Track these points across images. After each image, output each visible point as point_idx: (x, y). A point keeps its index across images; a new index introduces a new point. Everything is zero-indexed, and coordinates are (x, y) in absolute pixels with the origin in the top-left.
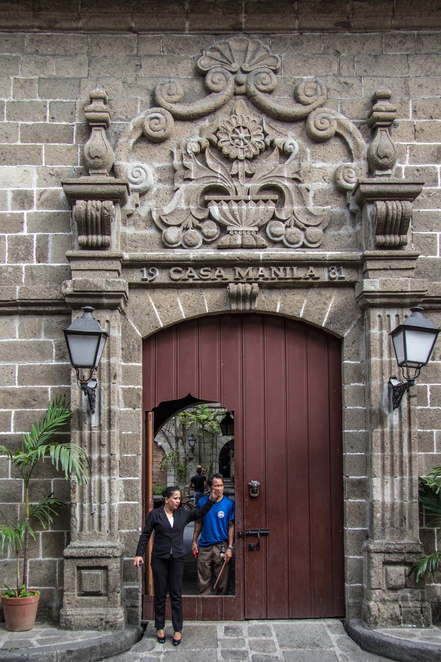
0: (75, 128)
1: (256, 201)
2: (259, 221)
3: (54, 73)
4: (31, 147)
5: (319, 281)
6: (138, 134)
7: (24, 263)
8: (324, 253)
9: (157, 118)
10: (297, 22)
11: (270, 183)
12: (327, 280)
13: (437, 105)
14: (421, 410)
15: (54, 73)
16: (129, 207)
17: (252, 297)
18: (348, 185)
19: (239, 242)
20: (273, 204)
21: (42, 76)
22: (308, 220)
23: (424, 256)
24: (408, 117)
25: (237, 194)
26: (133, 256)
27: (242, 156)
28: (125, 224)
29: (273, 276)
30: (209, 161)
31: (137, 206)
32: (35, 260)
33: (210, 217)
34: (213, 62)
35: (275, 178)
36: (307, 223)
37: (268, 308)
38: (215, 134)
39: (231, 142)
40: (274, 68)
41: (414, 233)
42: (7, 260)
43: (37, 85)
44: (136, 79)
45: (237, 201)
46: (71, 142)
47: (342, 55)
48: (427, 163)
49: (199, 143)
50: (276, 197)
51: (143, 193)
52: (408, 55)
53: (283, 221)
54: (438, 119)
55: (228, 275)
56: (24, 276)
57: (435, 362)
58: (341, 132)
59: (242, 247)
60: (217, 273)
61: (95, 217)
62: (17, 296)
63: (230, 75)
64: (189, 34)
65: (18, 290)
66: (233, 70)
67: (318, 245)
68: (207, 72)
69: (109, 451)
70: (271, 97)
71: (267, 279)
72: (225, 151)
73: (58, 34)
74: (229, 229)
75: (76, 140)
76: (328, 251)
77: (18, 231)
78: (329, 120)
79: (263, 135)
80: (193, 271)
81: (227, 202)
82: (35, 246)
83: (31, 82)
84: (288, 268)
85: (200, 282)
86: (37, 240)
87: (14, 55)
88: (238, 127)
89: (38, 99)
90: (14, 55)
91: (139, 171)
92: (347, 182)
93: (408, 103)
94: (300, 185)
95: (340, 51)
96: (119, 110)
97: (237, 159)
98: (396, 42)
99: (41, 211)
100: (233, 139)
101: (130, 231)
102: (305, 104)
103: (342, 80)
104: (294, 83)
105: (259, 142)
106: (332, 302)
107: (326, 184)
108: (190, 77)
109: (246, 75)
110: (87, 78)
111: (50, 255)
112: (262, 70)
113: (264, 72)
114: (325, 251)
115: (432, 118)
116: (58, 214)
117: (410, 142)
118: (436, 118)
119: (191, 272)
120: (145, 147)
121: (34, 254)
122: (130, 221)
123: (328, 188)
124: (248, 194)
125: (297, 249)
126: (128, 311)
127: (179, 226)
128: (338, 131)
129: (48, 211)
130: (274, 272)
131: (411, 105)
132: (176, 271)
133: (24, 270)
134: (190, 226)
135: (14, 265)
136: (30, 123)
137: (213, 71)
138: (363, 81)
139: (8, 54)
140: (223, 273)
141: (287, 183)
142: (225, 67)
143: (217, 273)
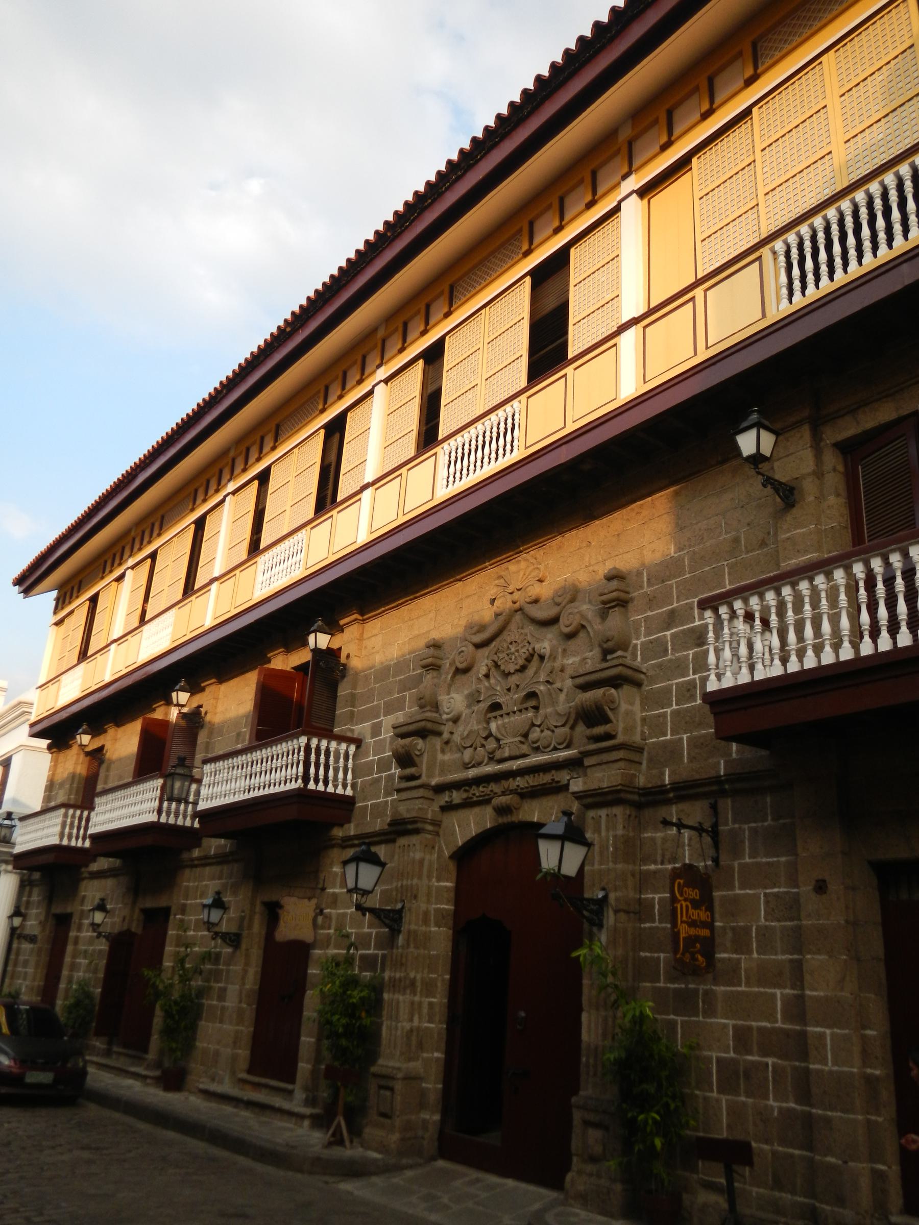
1: (520, 711)
2: (521, 731)
5: (561, 784)
6: (453, 669)
9: (462, 651)
13: (667, 567)
14: (650, 928)
15: (417, 632)
16: (446, 736)
19: (507, 754)
20: (533, 710)
23: (655, 740)
27: (512, 671)
28: (443, 751)
31: (452, 733)
33: (490, 735)
34: (499, 588)
38: (496, 654)
39: (507, 658)
45: (508, 714)
48: (659, 633)
49: (487, 665)
50: (533, 703)
51: (456, 720)
53: (539, 726)
55: (494, 787)
57: (664, 866)
58: (584, 623)
60: (490, 788)
62: (377, 828)
66: (510, 591)
67: (564, 745)
68: (494, 599)
69: (406, 971)
70: (537, 606)
71: (522, 789)
72: (502, 668)
79: (527, 644)
81: (501, 716)
84: (536, 775)
85: (481, 799)
88: (511, 643)
89: (408, 656)
93: (642, 574)
94: (554, 686)
95: (591, 541)
97: (509, 674)
98: (634, 514)
100: (508, 655)
101: (447, 757)
103: (591, 568)
109: (520, 592)
120: (461, 678)
122: (447, 749)
126: (441, 833)
127: (471, 746)
128: (582, 622)
131: (645, 575)
132: (466, 791)
136: (402, 677)
140: (494, 786)
141: (542, 688)
143: (490, 788)
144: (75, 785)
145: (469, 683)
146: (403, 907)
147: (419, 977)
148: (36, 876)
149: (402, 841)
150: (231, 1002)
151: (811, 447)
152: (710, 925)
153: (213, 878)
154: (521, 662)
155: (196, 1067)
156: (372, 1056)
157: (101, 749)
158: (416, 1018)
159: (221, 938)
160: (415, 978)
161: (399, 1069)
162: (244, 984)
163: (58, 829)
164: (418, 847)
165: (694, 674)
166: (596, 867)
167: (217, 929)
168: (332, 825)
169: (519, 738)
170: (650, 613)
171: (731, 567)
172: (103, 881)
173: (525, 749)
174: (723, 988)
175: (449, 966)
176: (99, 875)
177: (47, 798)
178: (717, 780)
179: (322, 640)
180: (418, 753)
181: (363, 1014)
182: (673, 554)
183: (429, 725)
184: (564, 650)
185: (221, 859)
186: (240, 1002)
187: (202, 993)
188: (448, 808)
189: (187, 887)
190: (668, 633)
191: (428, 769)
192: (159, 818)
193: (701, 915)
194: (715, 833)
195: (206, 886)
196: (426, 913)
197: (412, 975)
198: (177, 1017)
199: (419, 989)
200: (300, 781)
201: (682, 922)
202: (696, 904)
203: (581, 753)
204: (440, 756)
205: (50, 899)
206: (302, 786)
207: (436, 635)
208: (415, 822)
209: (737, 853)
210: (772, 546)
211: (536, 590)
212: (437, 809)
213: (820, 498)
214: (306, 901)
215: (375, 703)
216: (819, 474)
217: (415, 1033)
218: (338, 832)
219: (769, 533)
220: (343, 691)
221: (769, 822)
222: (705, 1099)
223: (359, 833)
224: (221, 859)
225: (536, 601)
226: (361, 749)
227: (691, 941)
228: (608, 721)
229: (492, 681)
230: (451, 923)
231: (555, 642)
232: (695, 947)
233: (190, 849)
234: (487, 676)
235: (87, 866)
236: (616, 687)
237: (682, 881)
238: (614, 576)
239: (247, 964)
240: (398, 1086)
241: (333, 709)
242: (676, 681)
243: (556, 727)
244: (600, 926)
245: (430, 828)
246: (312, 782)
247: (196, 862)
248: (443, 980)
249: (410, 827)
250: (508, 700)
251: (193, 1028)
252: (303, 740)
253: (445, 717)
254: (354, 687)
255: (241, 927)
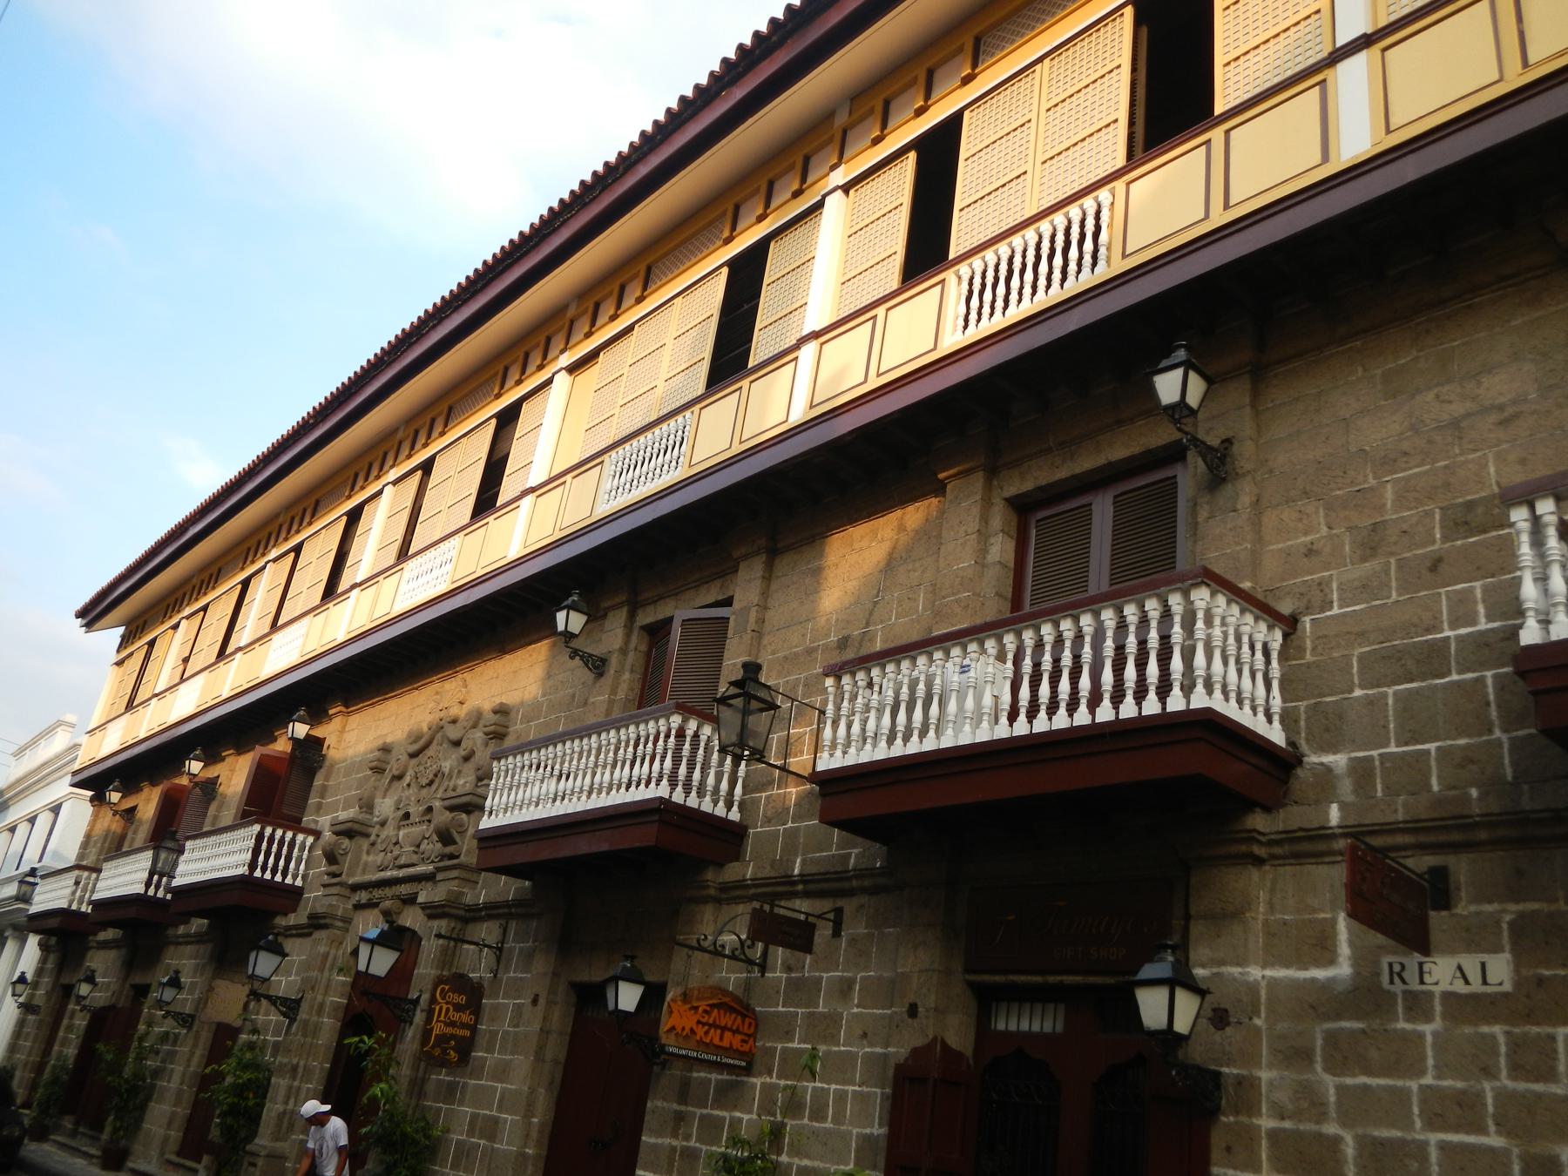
16: (373, 838)
31: (378, 836)
51: (383, 824)
55: (388, 892)
120: (396, 784)
144: (107, 845)
145: (397, 792)
146: (302, 997)
147: (302, 1063)
148: (53, 940)
149: (318, 935)
150: (174, 1084)
151: (625, 626)
152: (473, 1029)
153: (190, 958)
154: (431, 776)
155: (137, 1148)
156: (253, 1134)
157: (132, 810)
158: (292, 1102)
159: (173, 1017)
160: (298, 1063)
161: (265, 1147)
162: (189, 1066)
163: (68, 891)
164: (324, 941)
166: (421, 971)
167: (171, 1008)
168: (274, 914)
169: (413, 849)
171: (566, 718)
172: (108, 952)
173: (415, 858)
174: (473, 1082)
175: (331, 1056)
176: (104, 945)
177: (81, 856)
178: (506, 904)
179: (301, 730)
180: (342, 852)
181: (251, 1095)
183: (356, 827)
184: (459, 772)
185: (199, 939)
186: (181, 1084)
187: (156, 1073)
188: (358, 907)
189: (169, 964)
191: (349, 868)
192: (146, 891)
193: (466, 1018)
194: (500, 950)
195: (184, 964)
196: (322, 1005)
197: (295, 1061)
198: (125, 1096)
199: (300, 1075)
200: (246, 867)
201: (437, 1021)
202: (458, 1008)
203: (436, 868)
204: (364, 857)
205: (60, 968)
206: (247, 873)
207: (389, 740)
208: (324, 917)
209: (507, 970)
211: (455, 711)
212: (350, 907)
213: (619, 672)
214: (240, 986)
216: (624, 651)
217: (288, 1116)
220: (318, 782)
221: (530, 944)
222: (443, 1173)
224: (199, 939)
225: (454, 721)
227: (443, 1039)
228: (455, 843)
229: (411, 791)
230: (341, 1015)
231: (455, 764)
232: (448, 1043)
233: (176, 926)
234: (409, 785)
235: (95, 934)
236: (468, 813)
237: (447, 987)
238: (502, 711)
239: (195, 1046)
240: (260, 1162)
241: (306, 799)
244: (411, 1023)
245: (339, 924)
246: (259, 869)
247: (181, 940)
248: (322, 1069)
249: (322, 921)
250: (416, 810)
251: (143, 1108)
252: (257, 828)
253: (375, 819)
254: (327, 778)
255: (196, 1010)
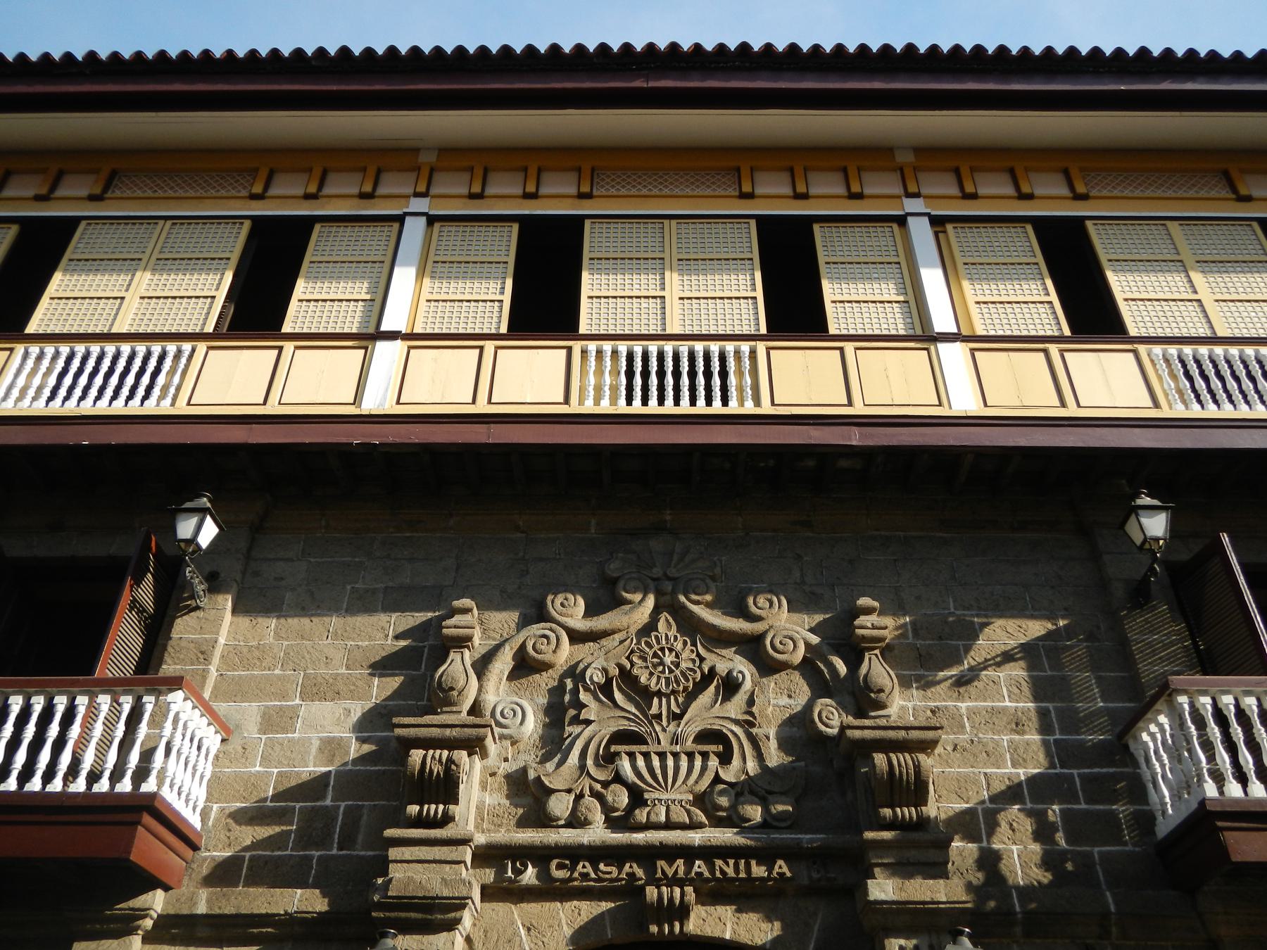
0: (426, 650)
3: (408, 581)
4: (359, 676)
7: (317, 851)
8: (800, 836)
10: (740, 519)
11: (709, 727)
12: (806, 882)
15: (408, 581)
17: (682, 912)
18: (828, 730)
21: (391, 584)
22: (770, 783)
24: (908, 639)
25: (659, 743)
26: (493, 839)
29: (718, 874)
30: (618, 696)
32: (335, 845)
33: (618, 779)
35: (717, 720)
36: (768, 788)
37: (711, 930)
40: (711, 574)
41: (940, 805)
42: (291, 845)
43: (381, 595)
44: (519, 588)
46: (418, 669)
47: (805, 559)
49: (605, 671)
50: (721, 747)
52: (895, 560)
54: (952, 640)
56: (313, 872)
59: (669, 825)
61: (436, 770)
63: (649, 581)
64: (596, 533)
65: (298, 896)
66: (655, 576)
67: (789, 823)
73: (421, 534)
74: (646, 796)
75: (426, 666)
76: (806, 833)
77: (318, 800)
78: (791, 639)
80: (587, 864)
82: (339, 823)
83: (374, 591)
86: (344, 813)
87: (357, 560)
90: (357, 560)
91: (513, 710)
92: (827, 726)
96: (492, 627)
97: (659, 694)
99: (358, 768)
102: (758, 619)
104: (740, 593)
105: (691, 670)
106: (819, 921)
107: (795, 729)
108: (594, 585)
110: (452, 586)
111: (360, 838)
112: (695, 576)
113: (697, 578)
114: (801, 833)
115: (942, 640)
116: (384, 772)
117: (914, 671)
118: (947, 639)
119: (584, 867)
121: (336, 836)
123: (798, 735)
124: (677, 744)
125: (755, 830)
127: (569, 791)
129: (368, 768)
130: (720, 867)
133: (315, 861)
134: (587, 792)
135: (301, 853)
137: (627, 577)
138: (836, 590)
139: (350, 559)
140: (635, 865)
142: (645, 572)
165: (1014, 766)
170: (922, 672)
182: (952, 610)
190: (963, 706)
210: (1107, 643)
215: (277, 672)
218: (157, 902)
219: (1099, 628)
223: (217, 911)
226: (229, 747)
242: (985, 771)
243: (770, 793)
